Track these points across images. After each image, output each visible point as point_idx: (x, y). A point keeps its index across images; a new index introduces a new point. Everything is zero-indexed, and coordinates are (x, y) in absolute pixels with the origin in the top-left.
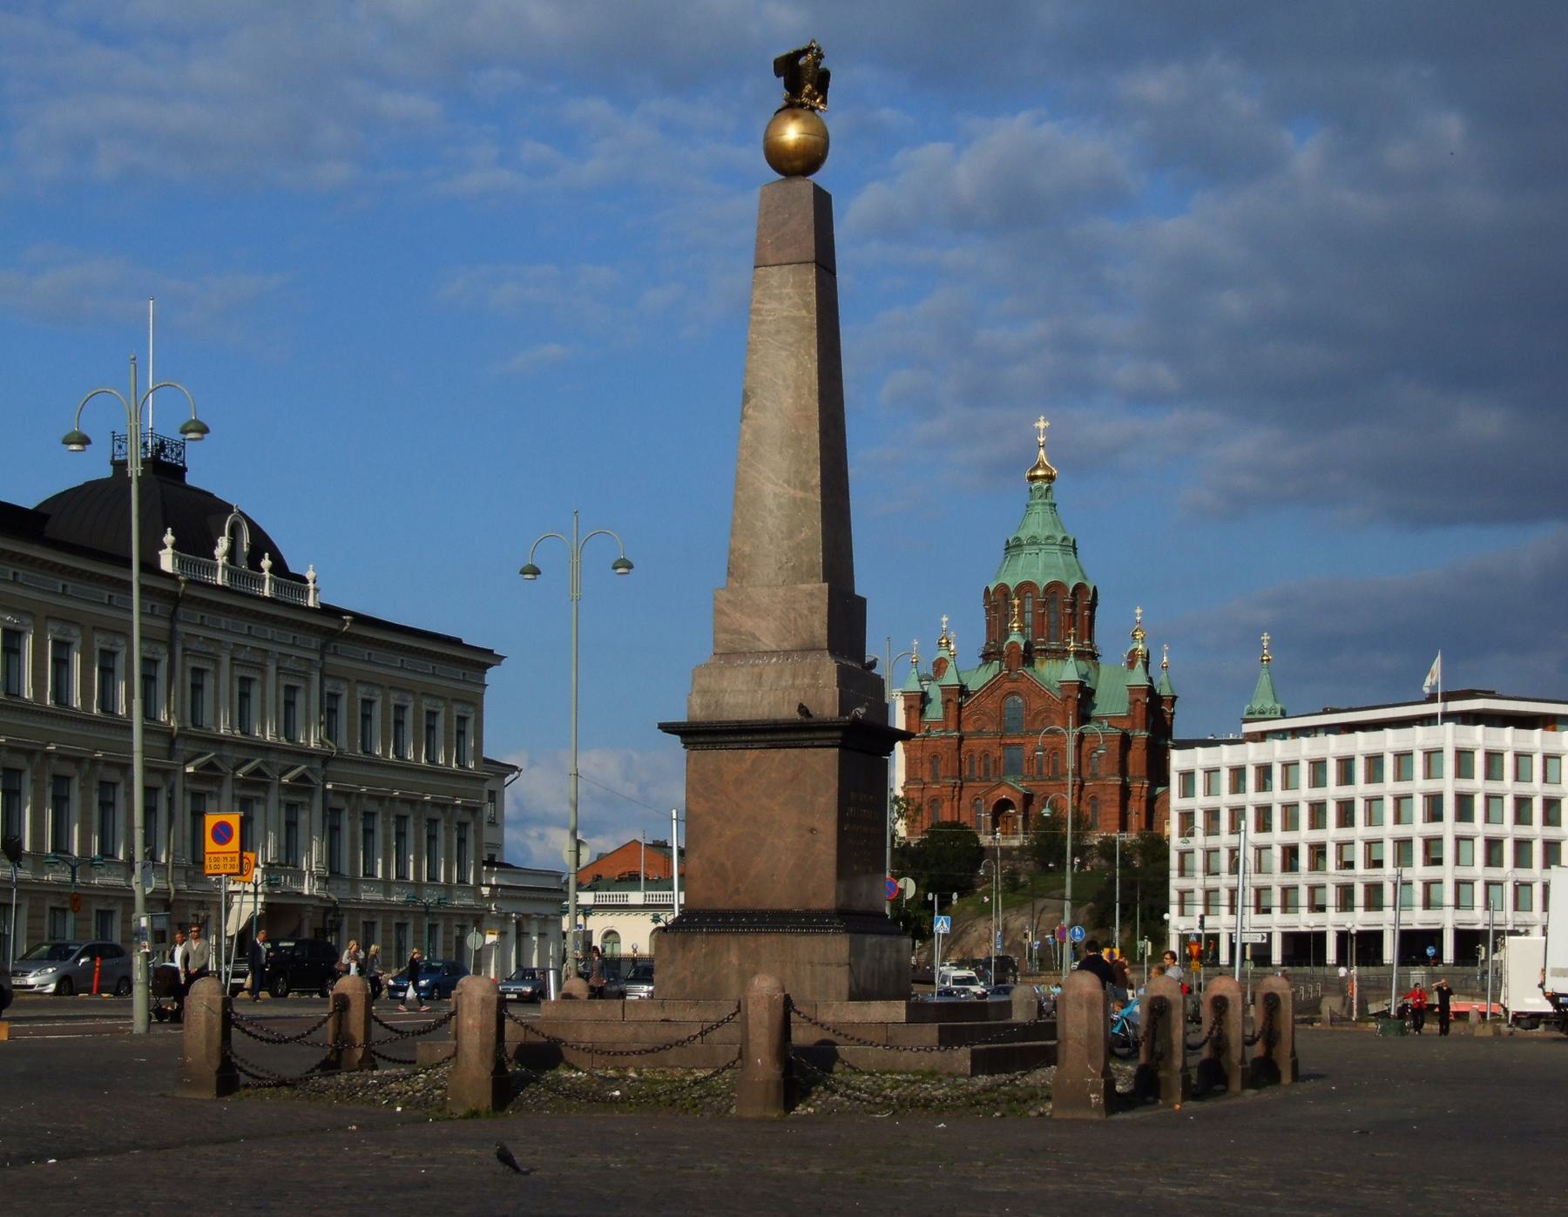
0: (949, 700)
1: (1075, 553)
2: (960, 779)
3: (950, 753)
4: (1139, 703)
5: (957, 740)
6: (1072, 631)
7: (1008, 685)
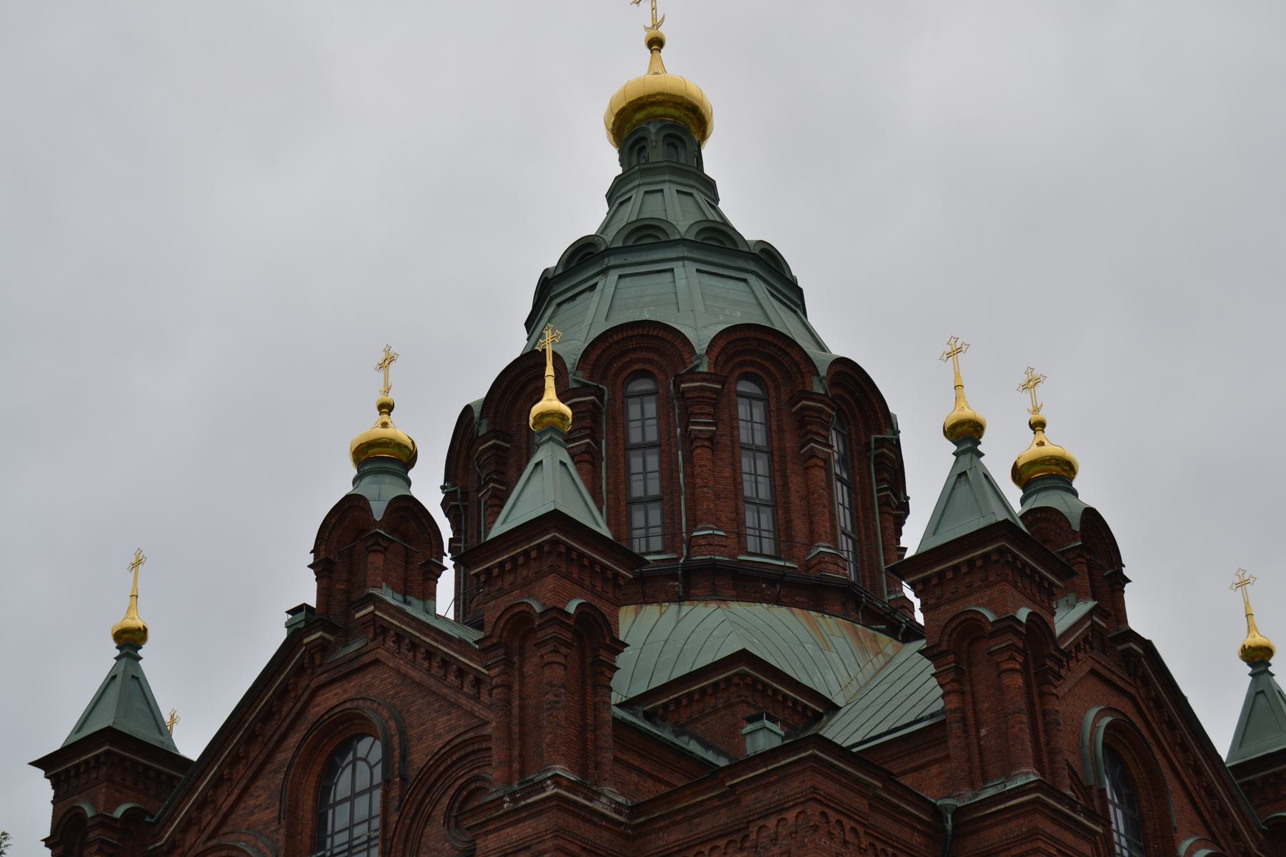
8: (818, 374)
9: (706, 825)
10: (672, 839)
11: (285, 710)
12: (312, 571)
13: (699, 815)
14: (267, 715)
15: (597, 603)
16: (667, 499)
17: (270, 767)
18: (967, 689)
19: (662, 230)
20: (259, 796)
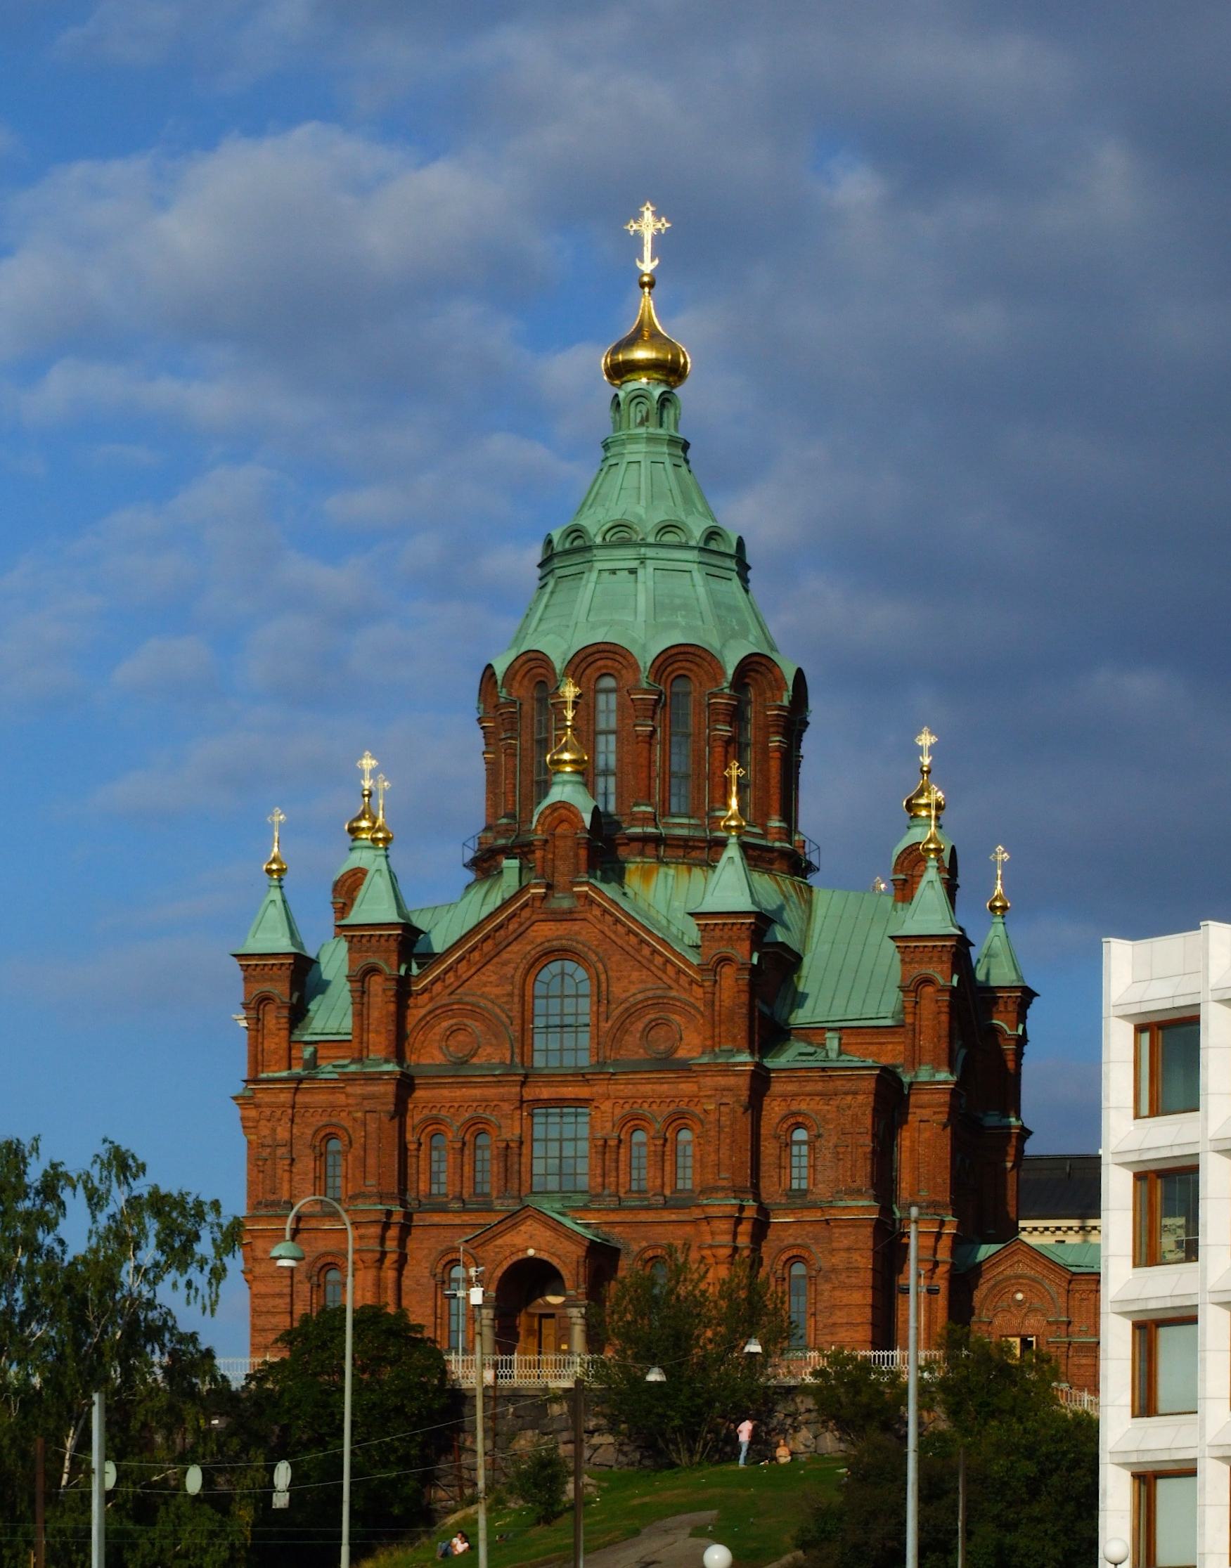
0: (372, 970)
1: (745, 581)
2: (403, 1203)
3: (372, 1126)
4: (929, 990)
5: (391, 1088)
6: (734, 771)
7: (545, 932)
8: (787, 690)
9: (809, 1088)
10: (789, 1088)
11: (511, 927)
13: (807, 1081)
14: (500, 927)
17: (496, 960)
18: (918, 1012)
20: (489, 976)
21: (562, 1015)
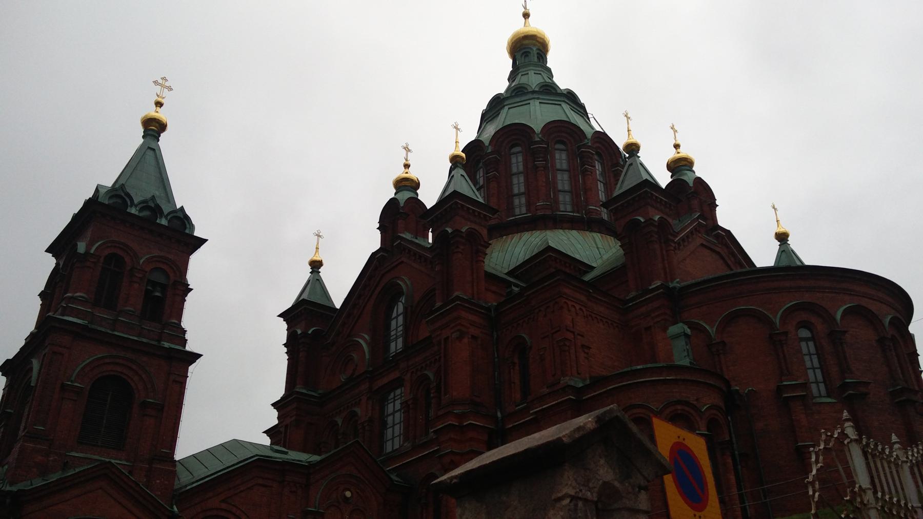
12: (378, 230)
15: (477, 228)
16: (527, 193)
19: (526, 89)
21: (396, 329)
